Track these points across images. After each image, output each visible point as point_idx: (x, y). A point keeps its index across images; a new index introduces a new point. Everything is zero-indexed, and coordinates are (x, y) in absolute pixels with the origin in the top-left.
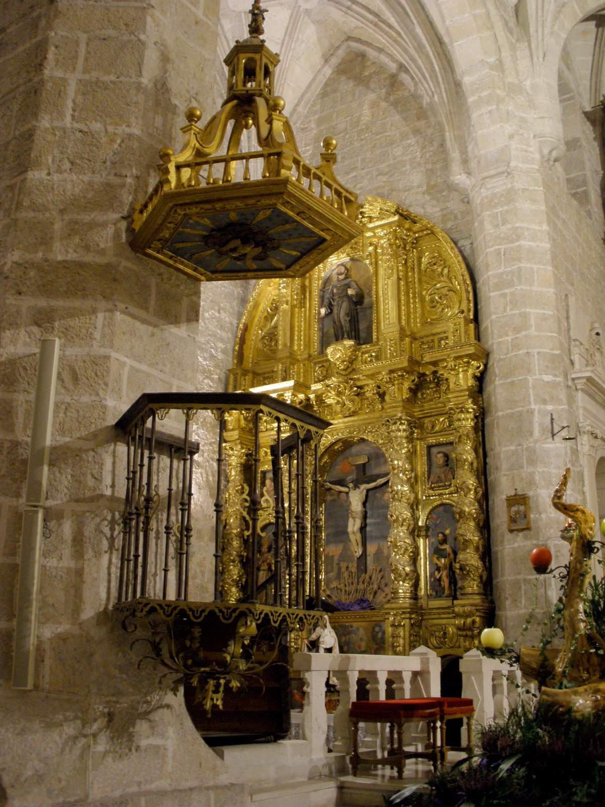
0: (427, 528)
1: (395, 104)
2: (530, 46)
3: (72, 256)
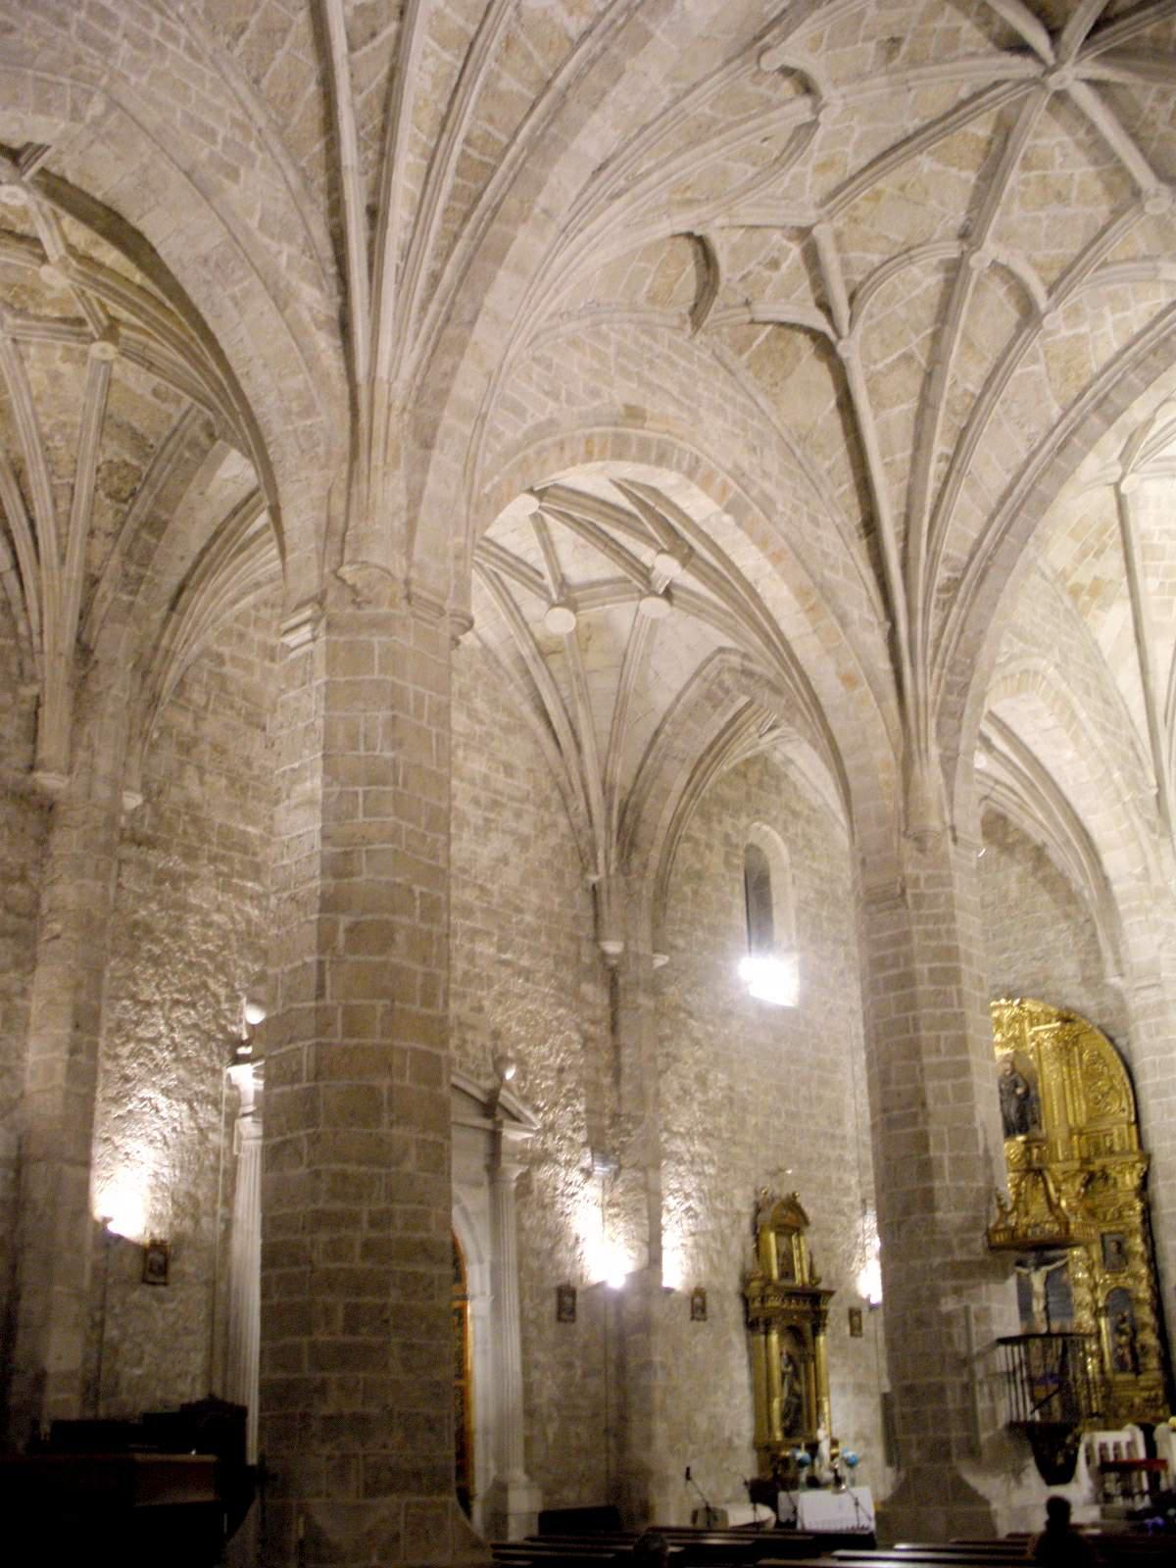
0: (1106, 1308)
1: (1044, 881)
2: (1172, 840)
3: (965, 1258)
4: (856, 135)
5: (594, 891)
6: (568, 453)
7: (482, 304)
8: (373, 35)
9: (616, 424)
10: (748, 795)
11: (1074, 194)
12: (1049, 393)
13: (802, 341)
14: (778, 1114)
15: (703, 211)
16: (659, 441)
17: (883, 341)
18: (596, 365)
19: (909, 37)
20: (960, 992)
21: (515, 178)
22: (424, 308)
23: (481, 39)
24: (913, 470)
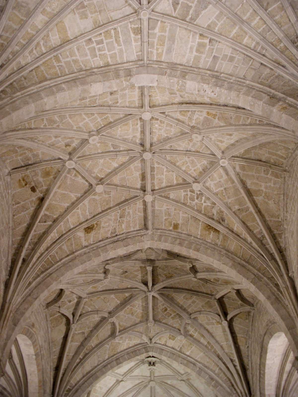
7: (39, 296)
8: (45, 222)
9: (29, 327)
12: (107, 352)
13: (64, 320)
16: (33, 334)
19: (129, 272)
21: (57, 270)
23: (65, 236)
24: (72, 359)
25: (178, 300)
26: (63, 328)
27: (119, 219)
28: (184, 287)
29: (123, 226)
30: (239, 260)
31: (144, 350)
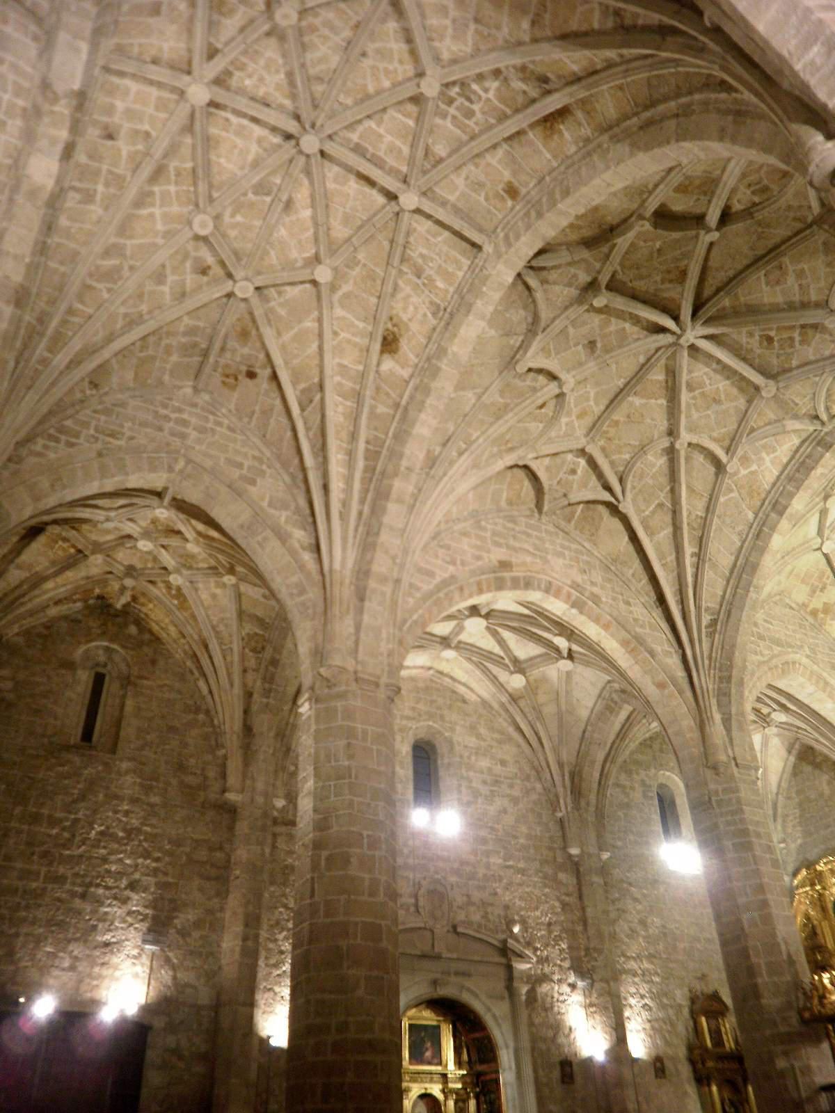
4: (592, 395)
5: (561, 820)
6: (466, 592)
8: (311, 401)
10: (654, 758)
11: (723, 397)
13: (601, 508)
14: (699, 940)
15: (520, 452)
17: (645, 500)
18: (479, 543)
19: (599, 340)
20: (754, 856)
22: (356, 530)
25: (766, 300)
26: (616, 524)
27: (419, 282)
28: (740, 267)
29: (440, 284)
30: (635, 119)
31: (819, 449)
